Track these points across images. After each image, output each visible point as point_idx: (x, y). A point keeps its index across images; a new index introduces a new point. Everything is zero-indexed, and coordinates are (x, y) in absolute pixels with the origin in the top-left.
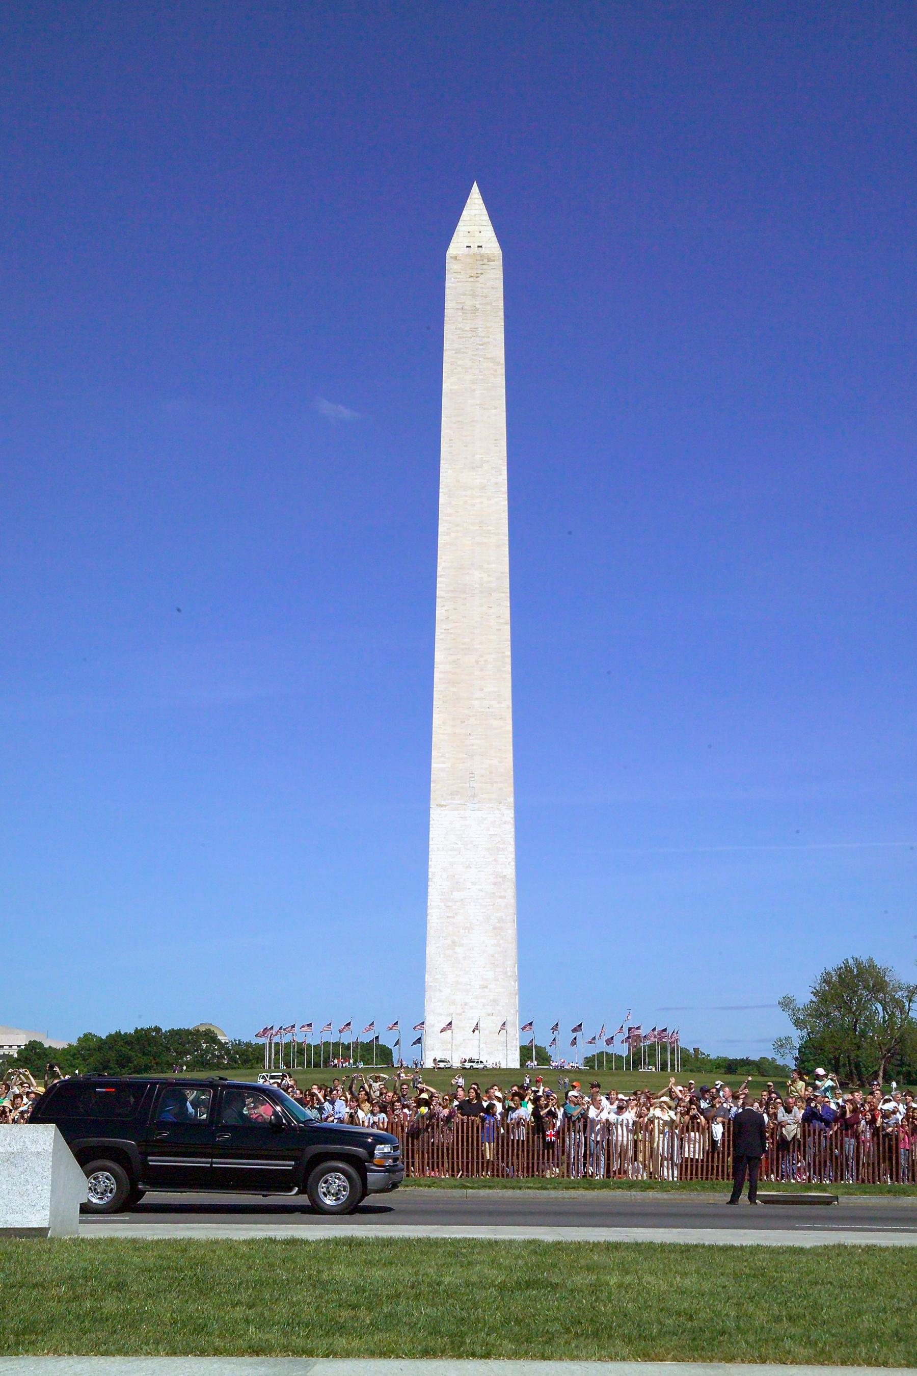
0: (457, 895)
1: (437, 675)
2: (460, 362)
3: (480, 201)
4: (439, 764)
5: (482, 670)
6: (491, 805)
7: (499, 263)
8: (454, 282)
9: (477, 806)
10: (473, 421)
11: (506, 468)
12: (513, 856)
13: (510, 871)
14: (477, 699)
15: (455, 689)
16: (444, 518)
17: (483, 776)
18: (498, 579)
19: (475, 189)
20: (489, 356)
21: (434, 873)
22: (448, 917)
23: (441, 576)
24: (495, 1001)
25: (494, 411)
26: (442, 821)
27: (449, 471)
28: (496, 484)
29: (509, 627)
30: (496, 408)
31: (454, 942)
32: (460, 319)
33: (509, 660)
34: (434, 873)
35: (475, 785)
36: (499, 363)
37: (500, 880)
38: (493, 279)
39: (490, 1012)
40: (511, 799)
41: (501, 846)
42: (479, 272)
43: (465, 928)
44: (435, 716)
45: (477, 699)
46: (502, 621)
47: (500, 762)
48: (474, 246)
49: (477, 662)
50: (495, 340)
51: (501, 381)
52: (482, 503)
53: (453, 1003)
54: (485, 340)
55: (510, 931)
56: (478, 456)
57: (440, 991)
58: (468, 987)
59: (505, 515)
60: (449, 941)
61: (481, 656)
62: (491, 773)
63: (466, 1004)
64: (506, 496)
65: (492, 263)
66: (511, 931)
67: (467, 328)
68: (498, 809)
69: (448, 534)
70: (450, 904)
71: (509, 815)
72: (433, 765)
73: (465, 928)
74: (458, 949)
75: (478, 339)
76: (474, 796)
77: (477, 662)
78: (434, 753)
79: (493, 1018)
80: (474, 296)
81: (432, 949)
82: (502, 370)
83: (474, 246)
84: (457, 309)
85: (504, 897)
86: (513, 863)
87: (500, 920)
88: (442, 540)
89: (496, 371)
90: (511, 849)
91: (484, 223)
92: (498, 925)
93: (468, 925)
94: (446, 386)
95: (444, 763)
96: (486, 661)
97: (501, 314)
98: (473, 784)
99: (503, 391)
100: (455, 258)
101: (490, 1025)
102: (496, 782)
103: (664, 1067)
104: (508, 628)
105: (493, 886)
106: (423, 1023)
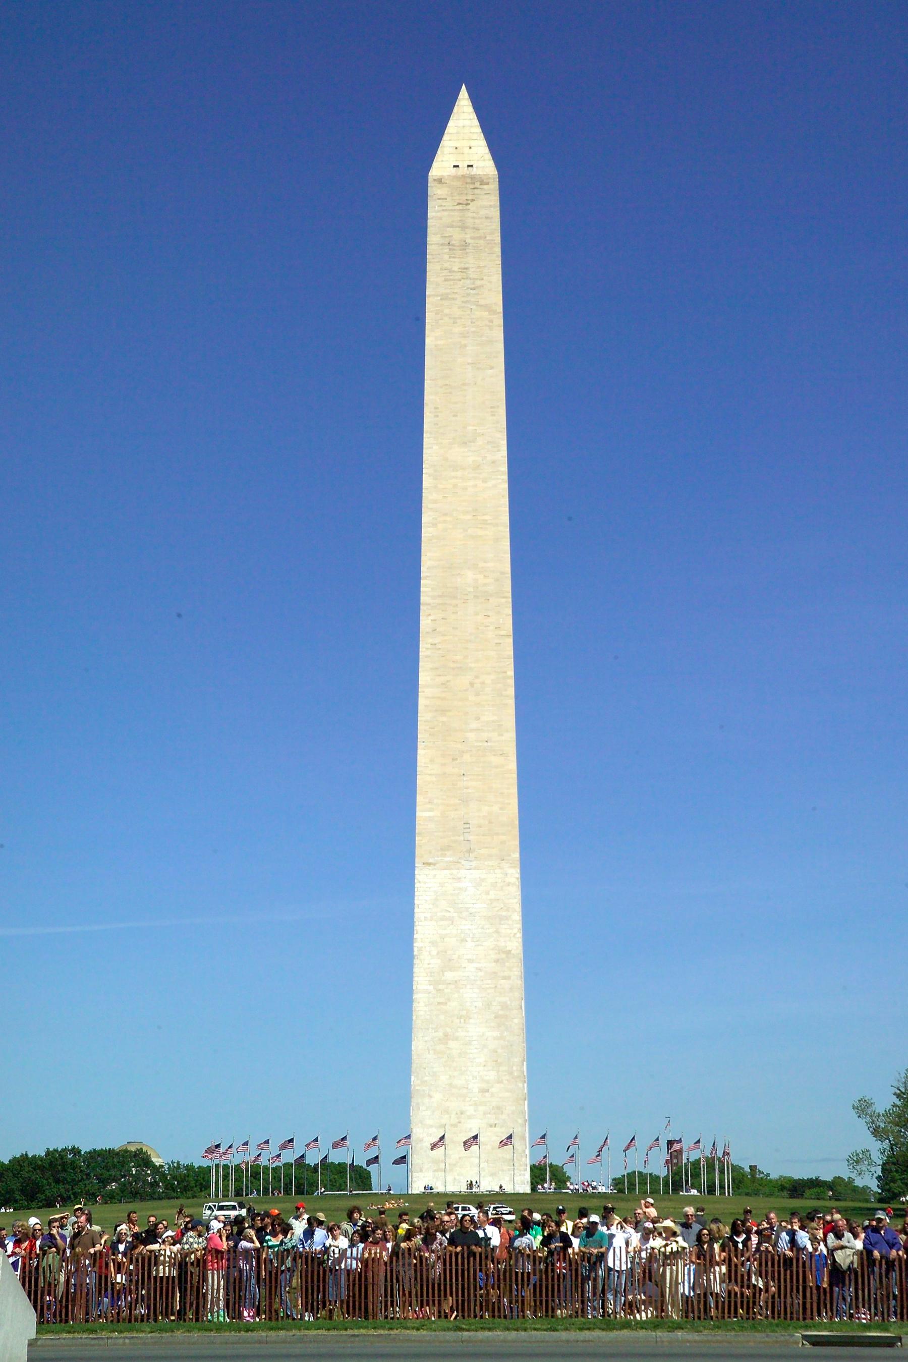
0: (449, 976)
1: (422, 702)
2: (446, 311)
3: (470, 109)
4: (428, 812)
5: (477, 695)
6: (491, 863)
7: (494, 186)
8: (439, 211)
9: (474, 864)
10: (464, 384)
11: (505, 442)
12: (520, 926)
13: (515, 945)
14: (471, 730)
15: (444, 719)
16: (430, 506)
17: (480, 826)
18: (497, 580)
19: (464, 94)
20: (482, 302)
21: (420, 949)
22: (439, 1003)
23: (426, 577)
24: (498, 1108)
25: (490, 372)
26: (429, 884)
27: (435, 447)
28: (494, 462)
29: (511, 640)
30: (492, 368)
31: (446, 1035)
32: (446, 257)
33: (512, 682)
34: (420, 949)
35: (471, 838)
36: (495, 312)
37: (504, 956)
38: (488, 207)
39: (492, 1122)
40: (517, 855)
41: (504, 914)
42: (470, 197)
44: (420, 752)
47: (501, 809)
48: (463, 165)
49: (472, 684)
50: (490, 282)
51: (498, 334)
52: (475, 486)
53: (447, 1111)
54: (478, 283)
55: (516, 1021)
56: (470, 428)
57: (430, 1096)
58: (465, 1091)
59: (505, 501)
60: (440, 1034)
61: (477, 677)
62: (490, 822)
64: (506, 477)
65: (485, 187)
66: (517, 1020)
67: (455, 269)
68: (500, 868)
69: (434, 525)
71: (514, 874)
72: (418, 814)
74: (452, 1044)
75: (468, 281)
76: (470, 851)
77: (472, 684)
78: (419, 799)
79: (497, 1129)
80: (463, 228)
81: (419, 1045)
82: (499, 321)
83: (463, 165)
84: (442, 244)
85: (509, 978)
86: (519, 935)
87: (504, 1006)
88: (427, 532)
89: (491, 321)
90: (517, 917)
91: (475, 136)
92: (501, 1013)
93: (464, 1013)
94: (429, 341)
95: (431, 810)
96: (483, 683)
97: (498, 250)
98: (468, 837)
99: (500, 346)
100: (440, 181)
101: (490, 1138)
102: (497, 834)
103: (711, 1191)
104: (510, 641)
105: (494, 964)
106: (409, 1137)
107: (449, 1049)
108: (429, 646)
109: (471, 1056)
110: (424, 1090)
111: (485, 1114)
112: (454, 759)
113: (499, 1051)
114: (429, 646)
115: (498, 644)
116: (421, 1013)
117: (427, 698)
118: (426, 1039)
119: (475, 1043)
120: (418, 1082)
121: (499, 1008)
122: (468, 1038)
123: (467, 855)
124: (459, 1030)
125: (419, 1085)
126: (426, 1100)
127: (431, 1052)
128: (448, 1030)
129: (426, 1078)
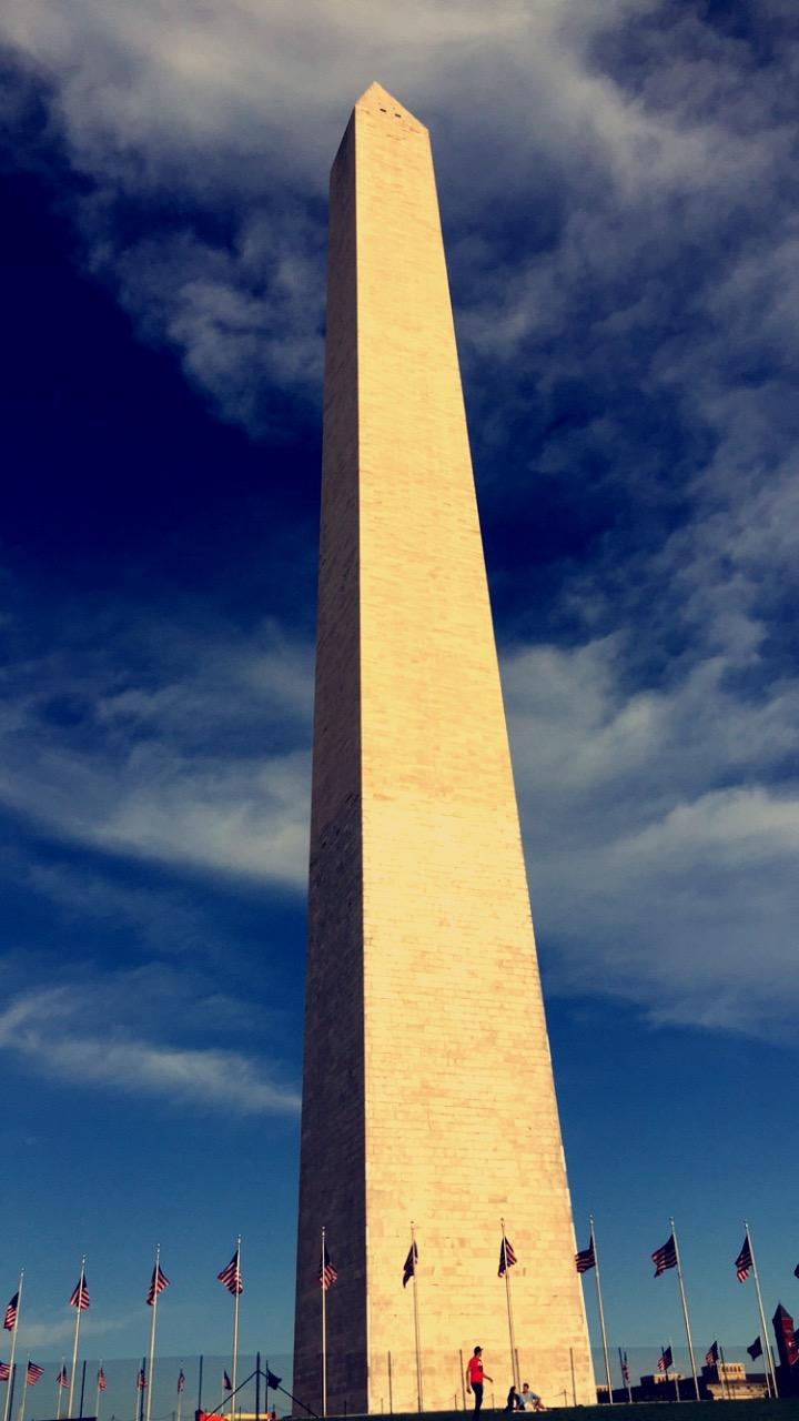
14: (435, 630)
22: (409, 1026)
23: (366, 444)
37: (508, 956)
43: (448, 1054)
45: (435, 630)
46: (469, 527)
52: (421, 371)
58: (465, 1198)
62: (472, 753)
63: (462, 1242)
70: (411, 997)
73: (448, 1054)
76: (445, 790)
92: (514, 1052)
93: (453, 1047)
108: (372, 518)
112: (414, 662)
114: (372, 518)
115: (463, 538)
117: (371, 577)
119: (476, 1104)
121: (511, 1044)
123: (441, 794)
127: (400, 1116)
129: (392, 1168)
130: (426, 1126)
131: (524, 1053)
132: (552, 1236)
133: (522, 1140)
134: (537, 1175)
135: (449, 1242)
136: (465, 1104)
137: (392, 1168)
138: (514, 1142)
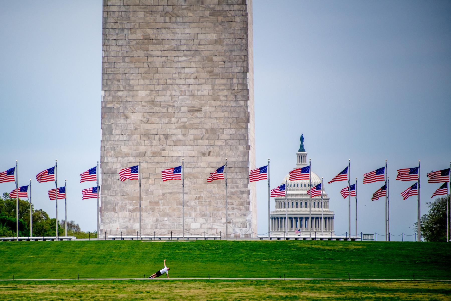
31: (147, 38)
43: (165, 14)
57: (126, 117)
58: (170, 110)
60: (139, 36)
74: (155, 51)
92: (218, 8)
107: (151, 55)
109: (179, 65)
110: (118, 109)
111: (195, 139)
113: (215, 59)
116: (114, 9)
118: (121, 42)
119: (185, 48)
120: (110, 98)
122: (174, 43)
124: (164, 31)
125: (111, 102)
126: (122, 121)
127: (127, 60)
128: (149, 31)
129: (120, 94)
130: (146, 65)
131: (226, 8)
132: (232, 131)
133: (216, 70)
134: (225, 93)
135: (157, 137)
136: (177, 48)
137: (120, 94)
138: (212, 72)
